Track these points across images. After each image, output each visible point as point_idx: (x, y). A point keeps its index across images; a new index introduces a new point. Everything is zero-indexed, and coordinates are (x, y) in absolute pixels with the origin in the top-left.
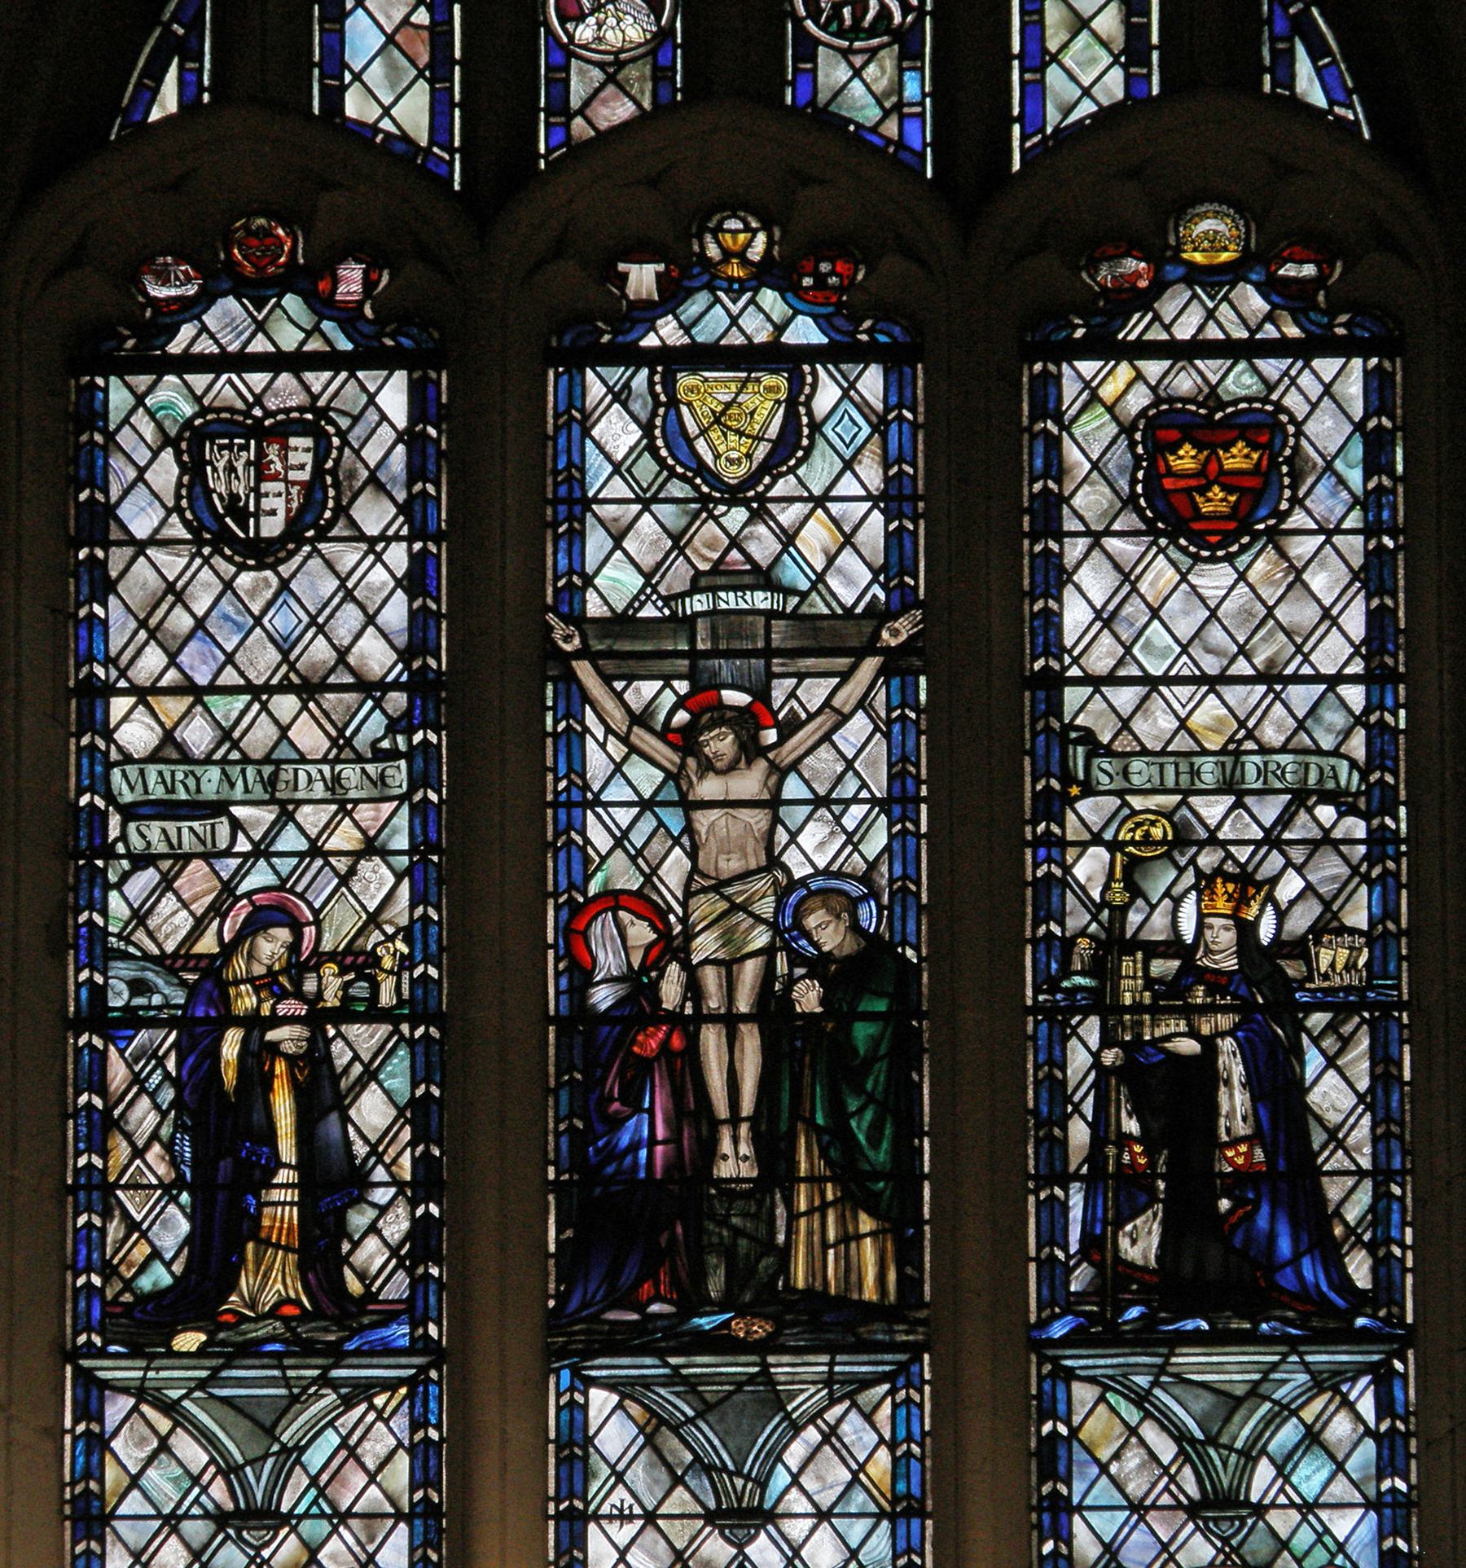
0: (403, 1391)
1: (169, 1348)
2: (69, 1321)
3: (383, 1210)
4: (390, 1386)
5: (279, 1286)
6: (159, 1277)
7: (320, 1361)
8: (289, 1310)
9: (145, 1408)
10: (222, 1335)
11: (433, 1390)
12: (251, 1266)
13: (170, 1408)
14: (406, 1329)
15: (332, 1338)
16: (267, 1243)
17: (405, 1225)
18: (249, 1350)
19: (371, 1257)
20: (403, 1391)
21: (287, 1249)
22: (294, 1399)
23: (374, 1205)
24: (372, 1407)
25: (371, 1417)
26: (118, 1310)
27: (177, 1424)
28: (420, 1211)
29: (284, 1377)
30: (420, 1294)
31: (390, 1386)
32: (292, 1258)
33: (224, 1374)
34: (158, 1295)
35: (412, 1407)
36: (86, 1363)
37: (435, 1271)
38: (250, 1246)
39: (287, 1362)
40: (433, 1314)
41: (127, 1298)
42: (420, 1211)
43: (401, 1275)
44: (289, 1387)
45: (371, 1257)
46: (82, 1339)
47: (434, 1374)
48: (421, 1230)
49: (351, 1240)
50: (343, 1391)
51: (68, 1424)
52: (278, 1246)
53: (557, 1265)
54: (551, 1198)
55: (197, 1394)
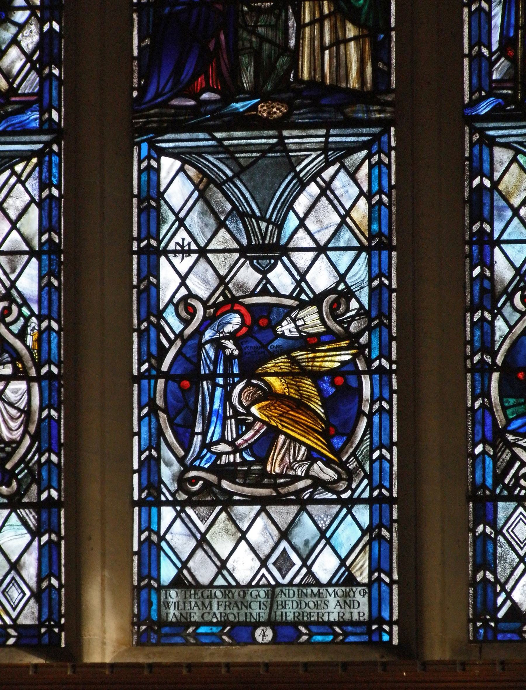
0: (35, 160)
3: (21, 27)
4: (25, 157)
11: (55, 159)
14: (36, 115)
17: (36, 38)
19: (13, 62)
20: (35, 160)
23: (15, 24)
24: (14, 173)
25: (13, 179)
28: (46, 28)
30: (46, 90)
31: (25, 157)
35: (40, 173)
37: (56, 72)
40: (55, 103)
42: (46, 28)
43: (33, 75)
45: (13, 62)
47: (55, 148)
48: (46, 40)
53: (139, 65)
54: (135, 16)
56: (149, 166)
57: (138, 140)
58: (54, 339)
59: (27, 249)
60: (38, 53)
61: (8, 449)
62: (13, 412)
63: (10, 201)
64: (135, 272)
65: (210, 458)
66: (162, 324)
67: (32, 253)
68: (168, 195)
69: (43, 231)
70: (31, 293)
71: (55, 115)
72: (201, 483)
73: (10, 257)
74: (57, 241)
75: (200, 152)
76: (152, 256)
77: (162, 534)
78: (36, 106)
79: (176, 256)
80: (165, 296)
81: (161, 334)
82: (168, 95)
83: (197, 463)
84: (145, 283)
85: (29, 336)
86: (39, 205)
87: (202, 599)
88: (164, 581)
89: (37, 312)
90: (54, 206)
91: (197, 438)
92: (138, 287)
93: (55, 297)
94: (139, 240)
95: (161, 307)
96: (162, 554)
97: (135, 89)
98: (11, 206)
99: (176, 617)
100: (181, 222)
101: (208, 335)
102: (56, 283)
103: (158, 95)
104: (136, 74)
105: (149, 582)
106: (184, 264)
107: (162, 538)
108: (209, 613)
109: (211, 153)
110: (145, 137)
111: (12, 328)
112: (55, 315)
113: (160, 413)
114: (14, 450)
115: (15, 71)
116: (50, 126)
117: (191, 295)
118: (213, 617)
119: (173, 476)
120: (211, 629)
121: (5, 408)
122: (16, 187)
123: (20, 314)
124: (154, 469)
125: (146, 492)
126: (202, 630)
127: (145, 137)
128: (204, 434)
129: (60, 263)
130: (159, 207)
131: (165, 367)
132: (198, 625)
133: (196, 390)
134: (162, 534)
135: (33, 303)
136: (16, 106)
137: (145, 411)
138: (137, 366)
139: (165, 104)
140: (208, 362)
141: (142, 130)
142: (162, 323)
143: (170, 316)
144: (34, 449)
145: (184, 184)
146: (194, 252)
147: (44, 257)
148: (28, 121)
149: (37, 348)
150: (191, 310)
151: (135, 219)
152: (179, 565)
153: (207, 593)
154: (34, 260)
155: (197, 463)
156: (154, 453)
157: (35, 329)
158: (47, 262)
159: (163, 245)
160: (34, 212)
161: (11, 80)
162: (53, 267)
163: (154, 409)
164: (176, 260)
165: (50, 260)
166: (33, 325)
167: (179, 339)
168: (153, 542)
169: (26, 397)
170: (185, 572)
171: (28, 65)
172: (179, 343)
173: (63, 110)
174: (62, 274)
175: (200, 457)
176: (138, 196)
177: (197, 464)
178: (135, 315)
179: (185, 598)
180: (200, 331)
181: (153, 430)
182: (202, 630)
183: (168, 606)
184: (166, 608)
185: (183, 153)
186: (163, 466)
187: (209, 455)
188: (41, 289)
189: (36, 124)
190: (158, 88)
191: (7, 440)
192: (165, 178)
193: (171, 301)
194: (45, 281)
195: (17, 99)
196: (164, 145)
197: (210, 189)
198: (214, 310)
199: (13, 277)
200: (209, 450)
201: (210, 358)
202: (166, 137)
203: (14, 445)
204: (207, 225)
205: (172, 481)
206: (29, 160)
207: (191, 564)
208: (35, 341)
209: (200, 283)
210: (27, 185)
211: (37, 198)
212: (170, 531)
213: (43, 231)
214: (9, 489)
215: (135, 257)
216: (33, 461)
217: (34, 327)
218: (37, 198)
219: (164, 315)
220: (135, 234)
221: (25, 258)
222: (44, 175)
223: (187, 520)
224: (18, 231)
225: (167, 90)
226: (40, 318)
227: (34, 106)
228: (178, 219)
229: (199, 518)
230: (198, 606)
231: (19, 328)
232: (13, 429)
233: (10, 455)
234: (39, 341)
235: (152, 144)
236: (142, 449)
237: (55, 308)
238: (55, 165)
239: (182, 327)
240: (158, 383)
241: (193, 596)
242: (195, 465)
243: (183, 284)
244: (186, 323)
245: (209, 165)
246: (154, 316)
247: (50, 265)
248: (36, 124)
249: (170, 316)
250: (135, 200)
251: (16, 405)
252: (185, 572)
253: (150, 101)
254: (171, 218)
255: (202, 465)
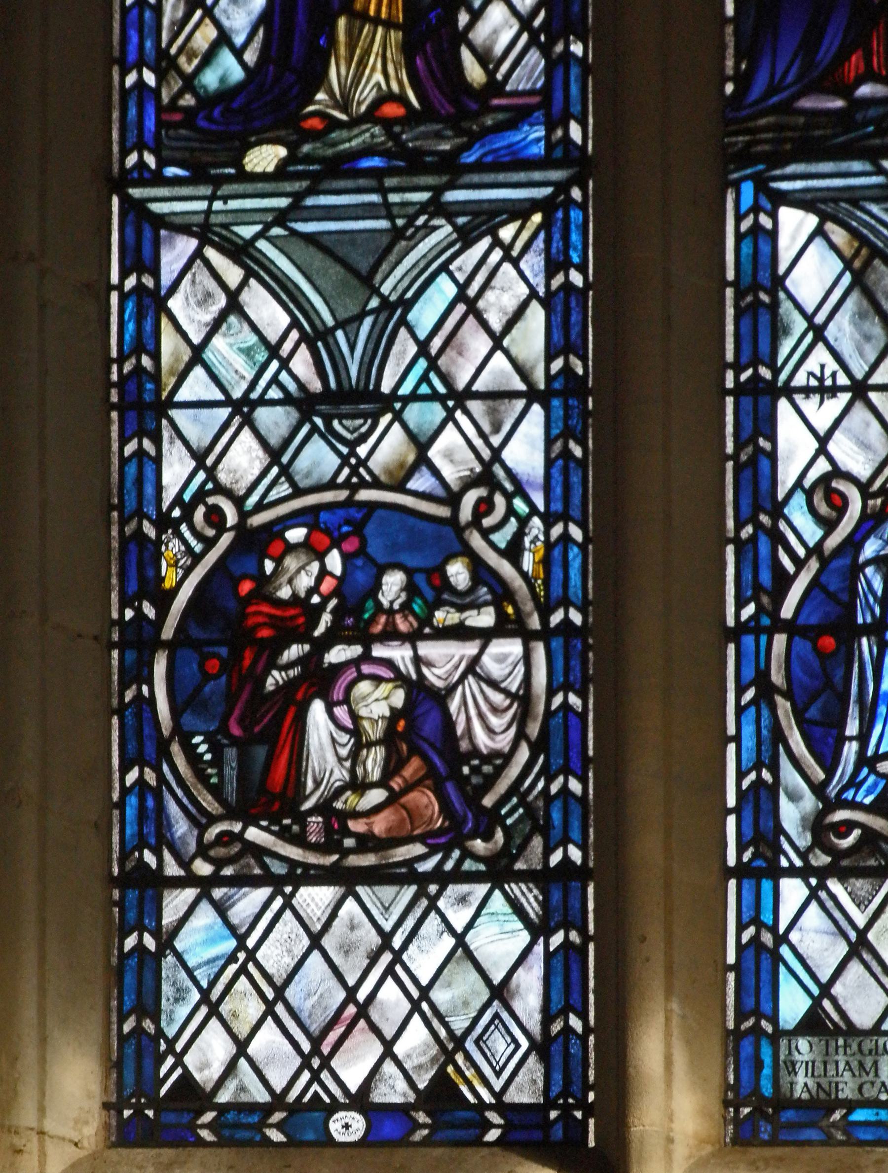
0: (537, 218)
1: (240, 167)
2: (115, 135)
4: (519, 212)
5: (378, 77)
6: (228, 69)
7: (430, 180)
8: (392, 110)
9: (211, 253)
10: (306, 148)
11: (576, 215)
12: (342, 50)
13: (240, 252)
14: (539, 132)
15: (446, 147)
16: (364, 17)
18: (338, 169)
19: (496, 32)
20: (537, 218)
21: (389, 24)
22: (397, 234)
24: (497, 242)
26: (177, 117)
27: (250, 273)
29: (386, 204)
31: (519, 212)
32: (395, 36)
33: (310, 201)
34: (227, 94)
35: (548, 242)
36: (136, 192)
37: (577, 49)
38: (342, 22)
39: (389, 182)
40: (576, 109)
41: (188, 100)
43: (534, 57)
44: (391, 217)
45: (496, 32)
46: (132, 159)
47: (576, 194)
49: (470, 10)
50: (461, 220)
51: (115, 278)
52: (376, 21)
53: (736, 33)
55: (276, 231)
56: (756, 227)
57: (735, 176)
58: (574, 558)
59: (522, 387)
60: (542, 14)
61: (487, 769)
62: (498, 698)
63: (490, 296)
64: (730, 429)
65: (875, 785)
66: (782, 528)
67: (532, 395)
68: (793, 282)
69: (552, 352)
70: (531, 472)
71: (575, 131)
72: (857, 832)
73: (490, 403)
74: (580, 371)
75: (855, 198)
76: (763, 398)
77: (781, 931)
78: (539, 115)
79: (807, 397)
80: (787, 475)
81: (780, 548)
82: (794, 89)
83: (849, 795)
84: (750, 449)
85: (526, 554)
86: (547, 303)
87: (858, 1057)
88: (785, 1021)
89: (541, 507)
90: (573, 304)
91: (850, 747)
92: (735, 457)
93: (575, 479)
94: (738, 368)
95: (780, 496)
96: (782, 969)
97: (729, 79)
98: (493, 305)
99: (809, 1091)
100: (819, 333)
101: (871, 548)
102: (578, 452)
103: (772, 89)
104: (730, 51)
105: (757, 1024)
106: (823, 413)
107: (782, 939)
108: (873, 1083)
109: (876, 200)
110: (749, 171)
111: (496, 537)
112: (576, 513)
113: (779, 699)
114: (499, 771)
115: (499, 48)
116: (566, 152)
117: (837, 472)
118: (880, 1092)
119: (804, 819)
120: (877, 1114)
121: (482, 691)
122: (502, 269)
123: (511, 511)
124: (765, 805)
125: (751, 850)
126: (859, 1115)
127: (749, 171)
128: (863, 738)
129: (585, 414)
130: (775, 304)
131: (787, 611)
132: (851, 1106)
133: (849, 654)
134: (781, 931)
135: (535, 489)
136: (501, 116)
137: (750, 694)
138: (733, 609)
139: (787, 108)
140: (871, 600)
141: (744, 158)
142: (782, 526)
143: (798, 513)
144: (536, 769)
145: (823, 259)
146: (844, 389)
147: (556, 403)
148: (523, 143)
149: (542, 576)
150: (838, 501)
151: (730, 328)
152: (816, 991)
153: (868, 1045)
154: (536, 408)
155: (849, 795)
156: (766, 775)
157: (539, 540)
158: (561, 413)
159: (783, 377)
160: (536, 315)
161: (491, 66)
162: (573, 422)
163: (766, 692)
164: (809, 406)
165: (567, 407)
166: (535, 532)
167: (814, 558)
168: (763, 946)
169: (521, 669)
170: (827, 1004)
171: (525, 37)
172: (814, 565)
173: (591, 120)
174: (590, 435)
175: (854, 783)
176: (735, 284)
177: (850, 797)
178: (730, 511)
179: (827, 1054)
180: (854, 542)
181: (765, 732)
182: (859, 1115)
183: (794, 1069)
184: (789, 1073)
185: (825, 201)
186: (783, 800)
187: (872, 779)
188: (549, 463)
189: (539, 150)
190: (773, 75)
191: (485, 751)
192: (788, 249)
193: (799, 484)
194: (558, 446)
195: (503, 101)
196: (785, 186)
197: (875, 270)
198: (882, 502)
199: (496, 441)
200: (873, 770)
201: (874, 594)
202: (791, 169)
203: (498, 762)
204: (868, 338)
205: (800, 829)
206: (525, 217)
207: (837, 989)
208: (539, 562)
209: (855, 448)
210: (523, 265)
211: (541, 291)
212: (798, 924)
213: (552, 352)
214: (490, 846)
215: (730, 401)
216: (535, 792)
217: (536, 537)
218: (541, 291)
219: (786, 511)
220: (730, 356)
221: (520, 404)
222: (555, 245)
223: (830, 904)
224: (507, 353)
225: (790, 78)
226: (549, 520)
227: (536, 114)
228: (811, 326)
229: (853, 900)
230: (851, 1069)
231: (509, 538)
232: (498, 730)
233: (490, 782)
234: (546, 562)
235: (761, 185)
236: (744, 768)
237: (576, 500)
238: (577, 226)
239: (820, 533)
240: (775, 642)
241: (841, 1051)
242: (846, 800)
243: (822, 450)
244: (829, 525)
245: (873, 222)
246: (766, 513)
247: (567, 417)
248: (539, 150)
249: (798, 513)
250: (729, 292)
251: (503, 685)
252: (827, 1004)
253: (757, 102)
254: (799, 325)
255: (859, 799)
